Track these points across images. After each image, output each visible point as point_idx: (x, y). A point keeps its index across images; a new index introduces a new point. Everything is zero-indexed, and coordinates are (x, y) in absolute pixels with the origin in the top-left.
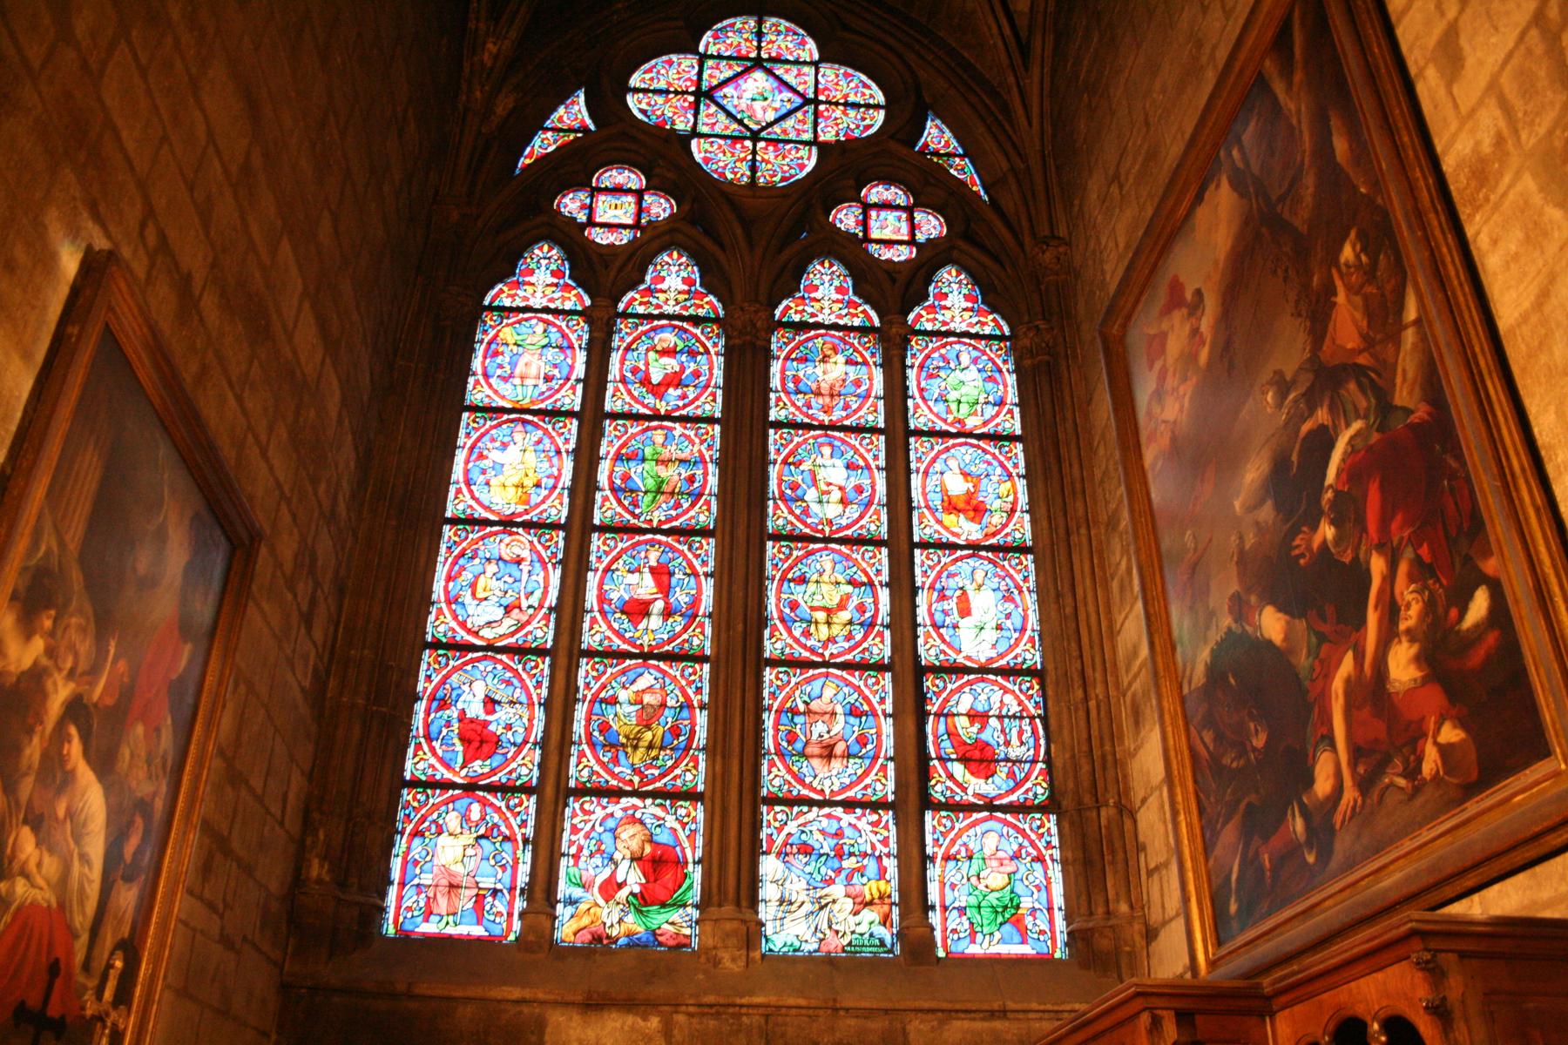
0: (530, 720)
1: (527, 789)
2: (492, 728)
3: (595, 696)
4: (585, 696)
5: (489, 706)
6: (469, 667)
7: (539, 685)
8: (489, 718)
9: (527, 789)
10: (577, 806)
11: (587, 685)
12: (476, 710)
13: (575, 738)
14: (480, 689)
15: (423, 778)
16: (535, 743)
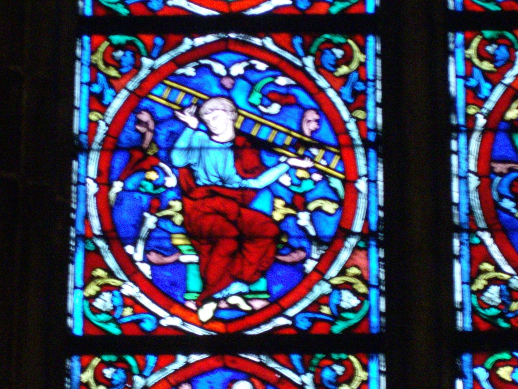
0: (349, 182)
1: (360, 342)
2: (262, 204)
3: (496, 117)
4: (471, 119)
5: (249, 156)
6: (190, 71)
7: (357, 102)
8: (252, 183)
9: (360, 342)
10: (482, 374)
11: (474, 96)
12: (218, 166)
13: (459, 217)
14: (221, 120)
15: (113, 329)
16: (366, 235)
